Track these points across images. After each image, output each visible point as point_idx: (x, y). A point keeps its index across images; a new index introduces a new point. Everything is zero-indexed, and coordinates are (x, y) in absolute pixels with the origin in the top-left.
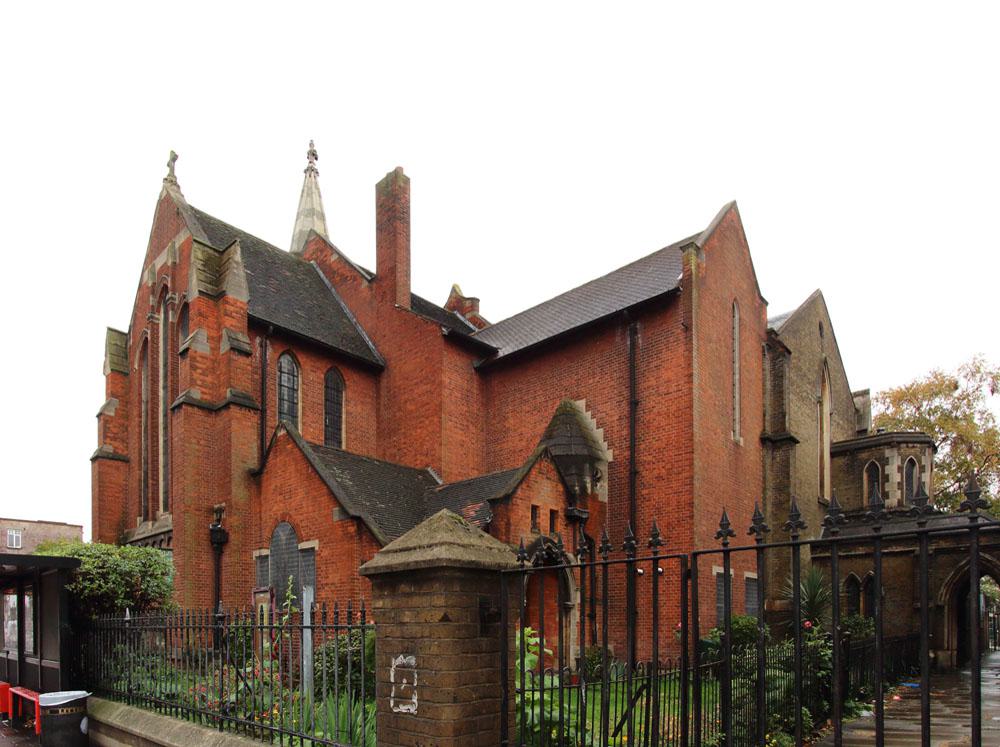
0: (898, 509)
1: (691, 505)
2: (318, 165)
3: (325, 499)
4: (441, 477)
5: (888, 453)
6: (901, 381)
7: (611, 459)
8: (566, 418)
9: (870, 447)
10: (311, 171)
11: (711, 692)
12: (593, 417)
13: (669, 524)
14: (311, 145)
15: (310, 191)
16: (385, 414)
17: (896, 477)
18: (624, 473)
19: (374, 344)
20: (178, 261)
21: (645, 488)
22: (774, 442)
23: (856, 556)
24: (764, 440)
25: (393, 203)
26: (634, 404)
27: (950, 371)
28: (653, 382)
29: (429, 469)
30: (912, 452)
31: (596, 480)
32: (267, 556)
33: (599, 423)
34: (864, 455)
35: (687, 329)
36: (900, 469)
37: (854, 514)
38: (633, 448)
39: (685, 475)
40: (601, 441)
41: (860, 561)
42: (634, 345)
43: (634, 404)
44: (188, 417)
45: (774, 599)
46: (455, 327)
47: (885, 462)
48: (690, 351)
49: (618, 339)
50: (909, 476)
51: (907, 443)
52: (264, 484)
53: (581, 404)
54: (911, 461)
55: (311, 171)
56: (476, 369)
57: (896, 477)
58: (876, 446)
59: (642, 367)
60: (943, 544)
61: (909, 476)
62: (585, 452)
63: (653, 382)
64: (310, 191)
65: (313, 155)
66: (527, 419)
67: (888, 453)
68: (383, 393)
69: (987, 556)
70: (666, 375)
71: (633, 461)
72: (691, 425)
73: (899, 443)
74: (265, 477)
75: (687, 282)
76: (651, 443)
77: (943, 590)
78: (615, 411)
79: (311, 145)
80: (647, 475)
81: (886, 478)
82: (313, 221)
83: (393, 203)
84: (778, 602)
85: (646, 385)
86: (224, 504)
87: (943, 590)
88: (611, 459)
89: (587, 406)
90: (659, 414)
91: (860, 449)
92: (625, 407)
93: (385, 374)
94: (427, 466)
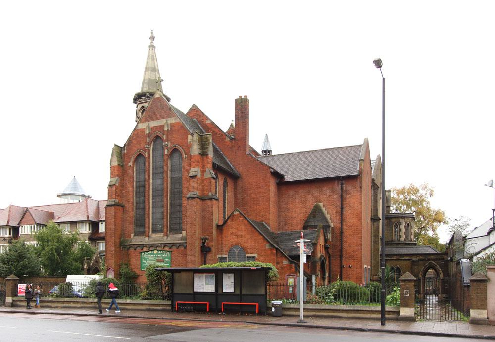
0: (405, 242)
1: (361, 245)
2: (155, 43)
3: (261, 241)
4: (269, 226)
5: (401, 220)
6: (400, 187)
7: (332, 226)
8: (316, 212)
9: (395, 217)
10: (152, 47)
11: (19, 303)
12: (326, 210)
13: (353, 251)
14: (152, 33)
15: (152, 58)
16: (240, 197)
17: (404, 230)
18: (338, 232)
19: (233, 166)
20: (170, 129)
21: (345, 238)
22: (374, 219)
23: (394, 260)
24: (371, 219)
25: (242, 107)
26: (342, 209)
27: (417, 185)
28: (348, 202)
29: (264, 222)
30: (408, 221)
31: (329, 233)
32: (226, 258)
33: (330, 213)
34: (393, 220)
35: (361, 187)
36: (405, 227)
37: (390, 243)
38: (341, 223)
39: (359, 235)
40: (329, 219)
41: (394, 261)
42: (342, 189)
43: (342, 209)
44: (197, 202)
45: (373, 275)
46: (260, 164)
47: (400, 224)
48: (361, 194)
49: (336, 184)
50: (408, 229)
51: (407, 217)
52: (224, 232)
53: (321, 204)
54: (408, 224)
55: (152, 47)
56: (277, 183)
57: (404, 230)
58: (397, 217)
59: (345, 197)
60: (421, 258)
61: (408, 229)
62: (327, 224)
63: (348, 202)
64: (152, 58)
65: (153, 38)
66: (299, 207)
67: (401, 220)
68: (239, 187)
69: (434, 263)
70: (353, 201)
71: (341, 228)
72: (361, 219)
73: (405, 217)
74: (225, 228)
75: (361, 172)
76: (347, 222)
77: (421, 273)
78: (335, 210)
79: (152, 33)
80: (346, 233)
81: (401, 230)
82: (155, 74)
83: (242, 107)
84: (375, 277)
85: (346, 203)
86: (208, 237)
87: (421, 273)
88: (332, 226)
89: (323, 206)
90: (350, 213)
91: (393, 218)
92: (339, 210)
93: (240, 180)
94: (263, 221)
